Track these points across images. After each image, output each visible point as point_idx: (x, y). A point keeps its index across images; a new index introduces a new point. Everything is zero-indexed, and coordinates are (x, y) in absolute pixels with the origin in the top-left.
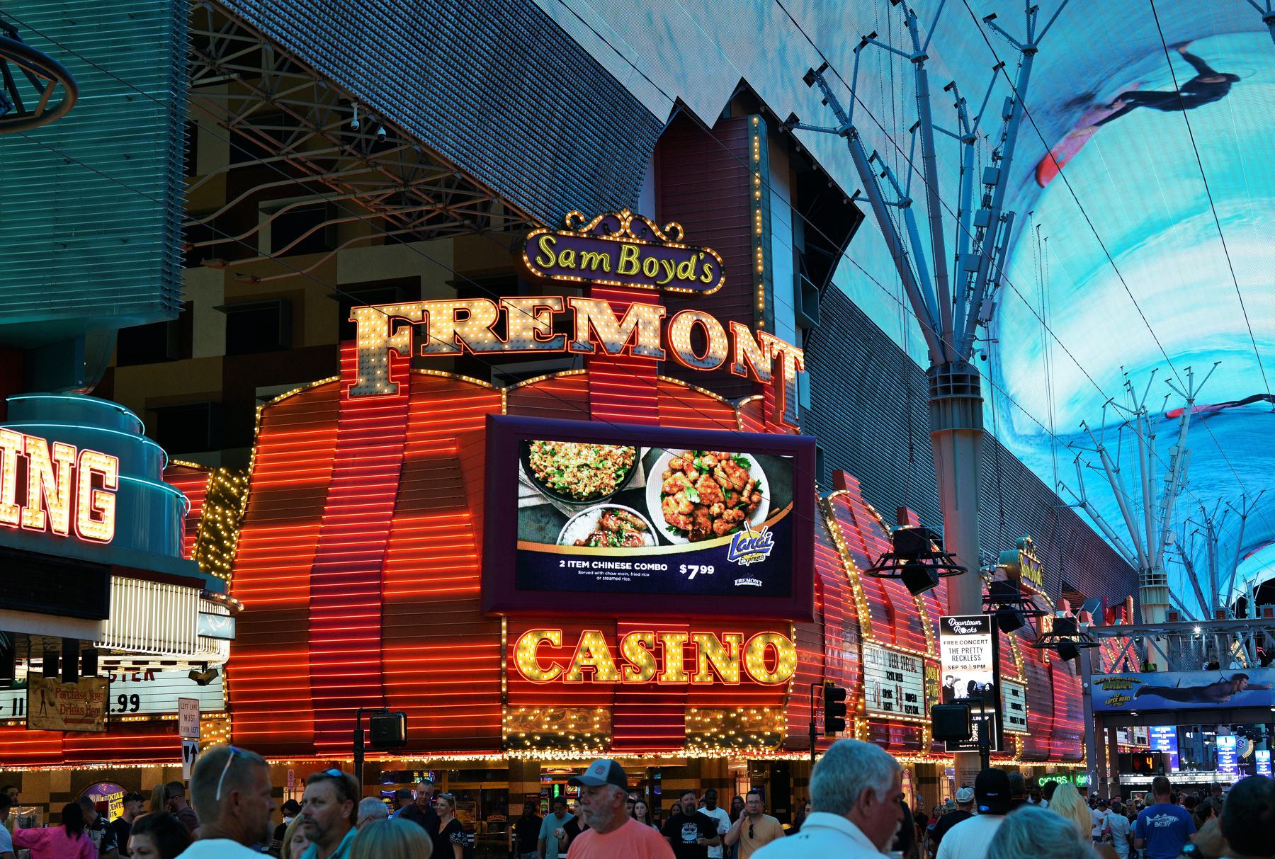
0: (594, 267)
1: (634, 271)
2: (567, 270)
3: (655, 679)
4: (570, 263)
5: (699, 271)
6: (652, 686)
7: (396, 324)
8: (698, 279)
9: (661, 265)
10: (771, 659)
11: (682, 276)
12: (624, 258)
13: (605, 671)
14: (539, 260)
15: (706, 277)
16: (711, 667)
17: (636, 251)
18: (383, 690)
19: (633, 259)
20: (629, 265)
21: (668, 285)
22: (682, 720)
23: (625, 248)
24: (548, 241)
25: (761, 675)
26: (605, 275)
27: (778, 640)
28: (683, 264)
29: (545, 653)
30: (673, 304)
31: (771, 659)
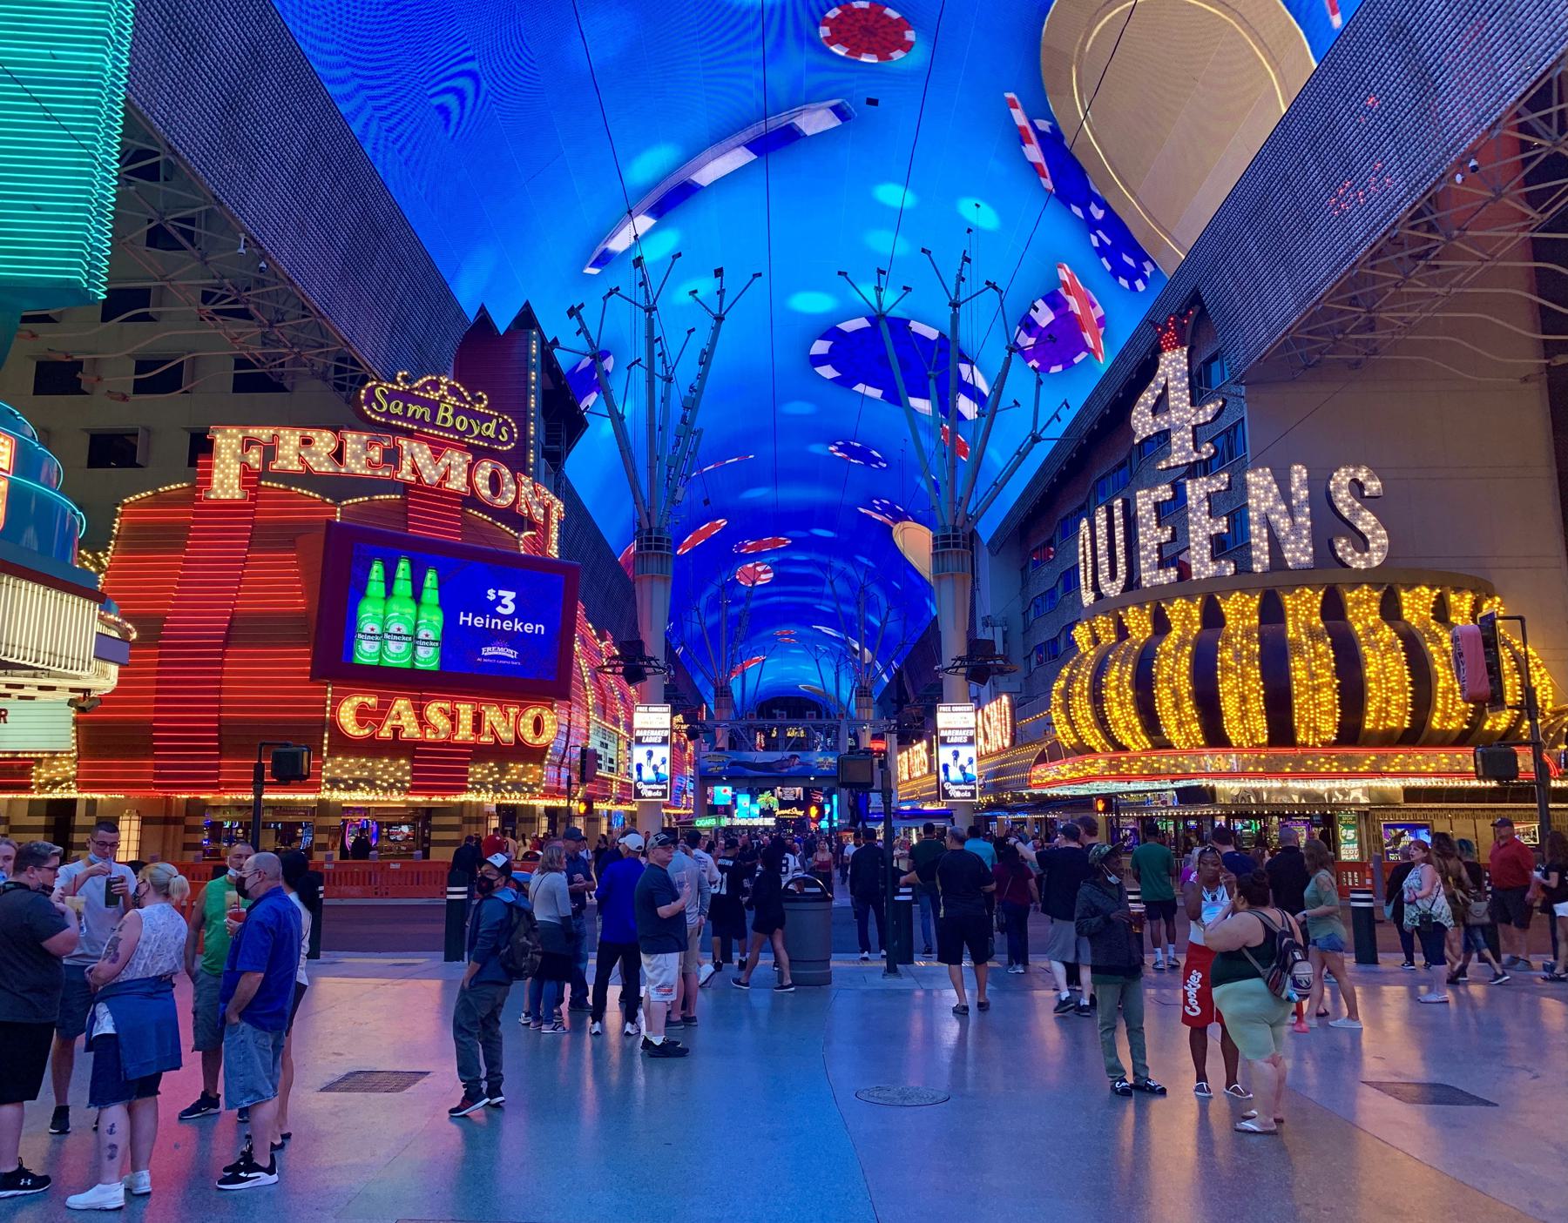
2: (396, 417)
4: (399, 411)
5: (498, 431)
7: (248, 443)
10: (538, 726)
12: (441, 414)
13: (411, 730)
14: (374, 406)
19: (449, 415)
20: (445, 419)
22: (466, 771)
23: (443, 406)
29: (362, 714)
30: (479, 454)
31: (538, 726)
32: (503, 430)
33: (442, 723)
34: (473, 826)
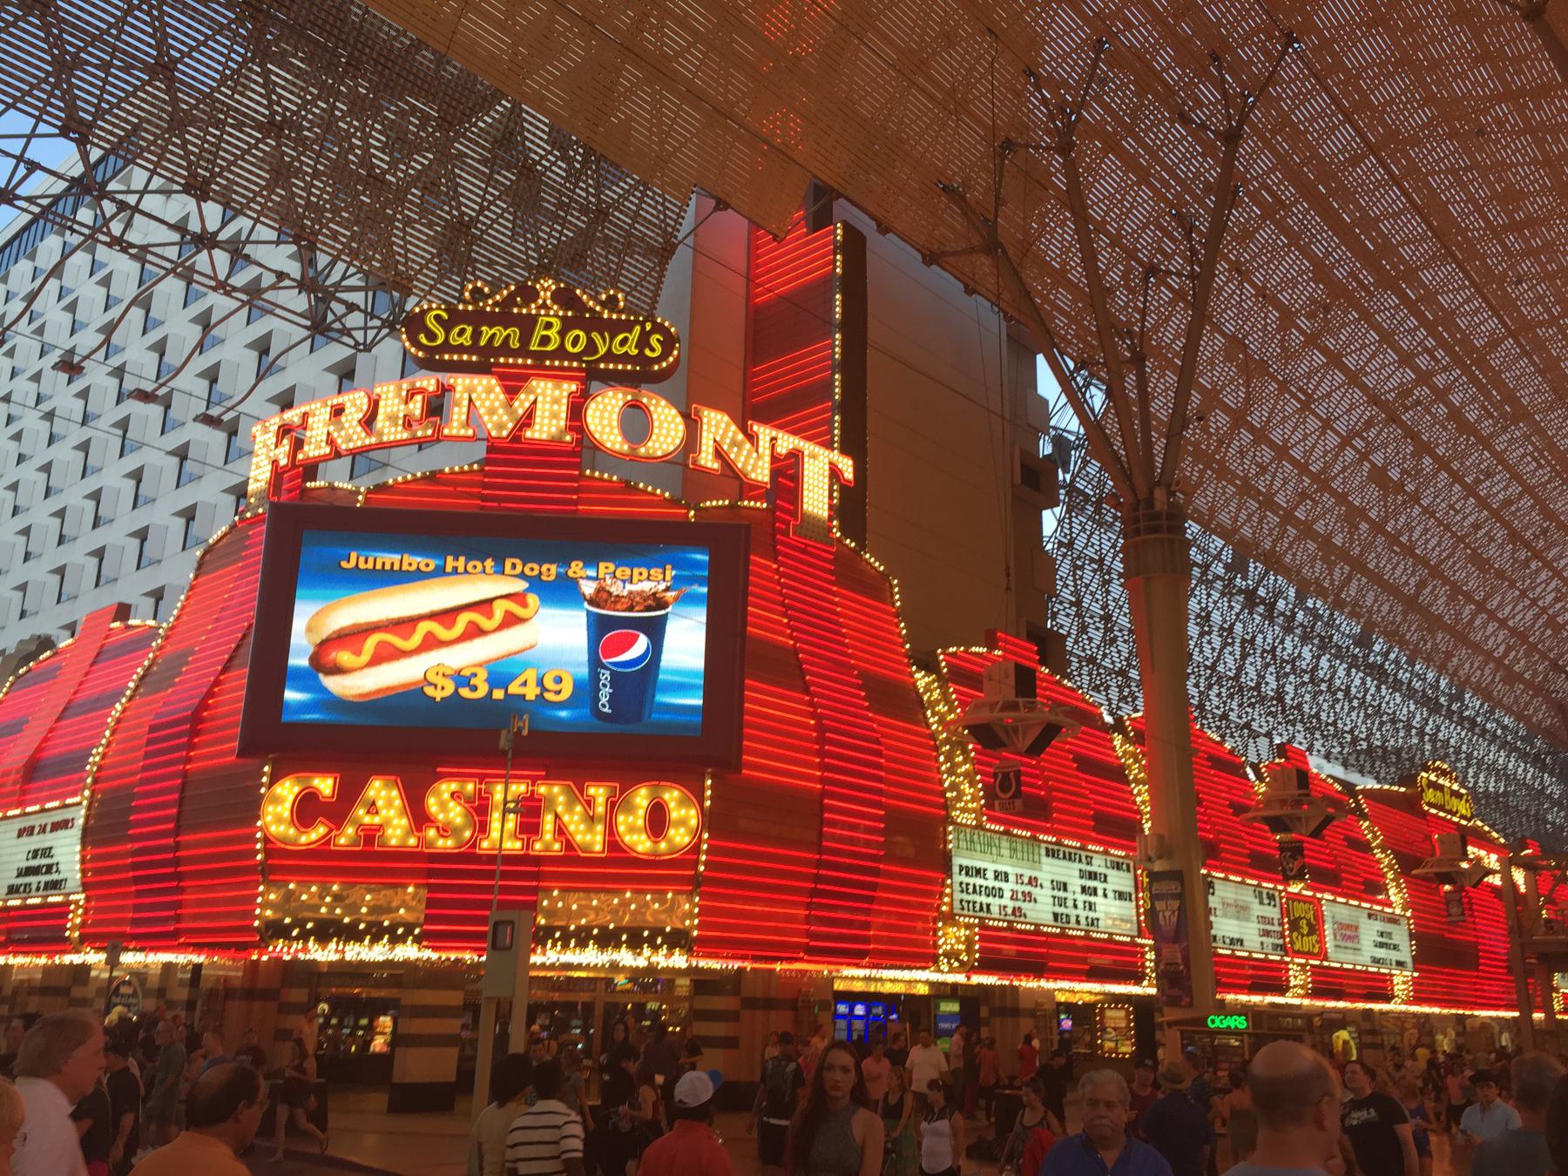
0: (497, 344)
1: (550, 348)
2: (461, 349)
3: (474, 846)
4: (466, 340)
5: (643, 342)
6: (468, 856)
8: (641, 353)
9: (591, 341)
10: (657, 821)
12: (540, 332)
14: (423, 339)
15: (653, 350)
16: (560, 831)
21: (601, 360)
24: (437, 318)
26: (515, 353)
27: (672, 796)
28: (621, 337)
29: (307, 809)
30: (592, 377)
31: (657, 821)
32: (654, 340)
33: (455, 814)
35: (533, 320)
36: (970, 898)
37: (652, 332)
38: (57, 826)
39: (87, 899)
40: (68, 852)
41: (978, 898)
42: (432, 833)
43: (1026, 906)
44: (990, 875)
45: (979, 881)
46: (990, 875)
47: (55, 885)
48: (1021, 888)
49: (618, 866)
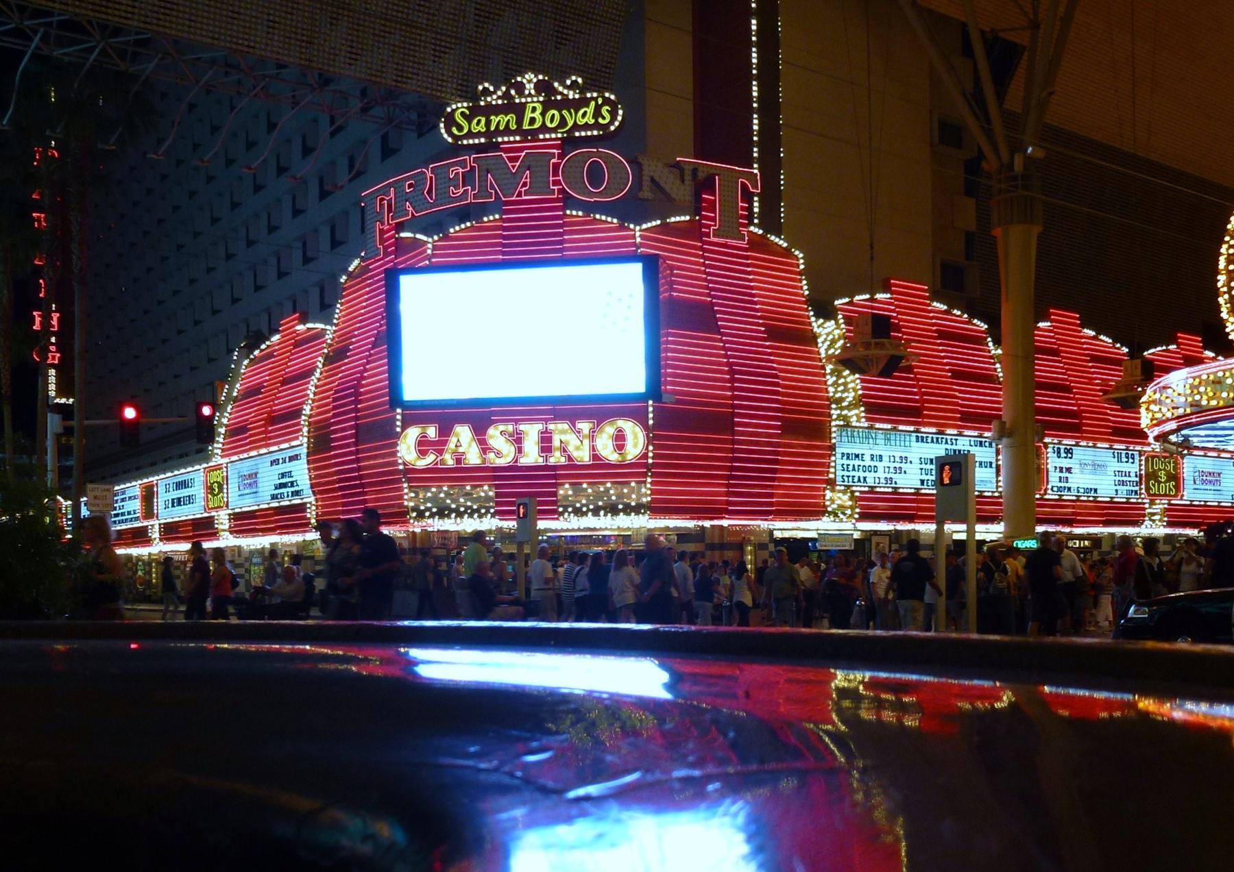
1: (536, 126)
4: (482, 128)
5: (598, 113)
6: (512, 468)
8: (596, 121)
9: (562, 117)
10: (620, 438)
11: (581, 122)
12: (528, 115)
13: (473, 457)
14: (454, 130)
15: (604, 118)
17: (539, 108)
18: (361, 477)
20: (533, 121)
22: (555, 494)
24: (463, 114)
25: (612, 457)
26: (513, 133)
29: (423, 445)
31: (620, 438)
34: (717, 553)
35: (523, 106)
36: (852, 474)
37: (603, 105)
38: (292, 459)
39: (317, 500)
40: (301, 473)
41: (856, 474)
42: (492, 456)
43: (896, 477)
44: (867, 458)
45: (857, 462)
46: (867, 458)
47: (297, 493)
48: (892, 465)
49: (599, 469)
